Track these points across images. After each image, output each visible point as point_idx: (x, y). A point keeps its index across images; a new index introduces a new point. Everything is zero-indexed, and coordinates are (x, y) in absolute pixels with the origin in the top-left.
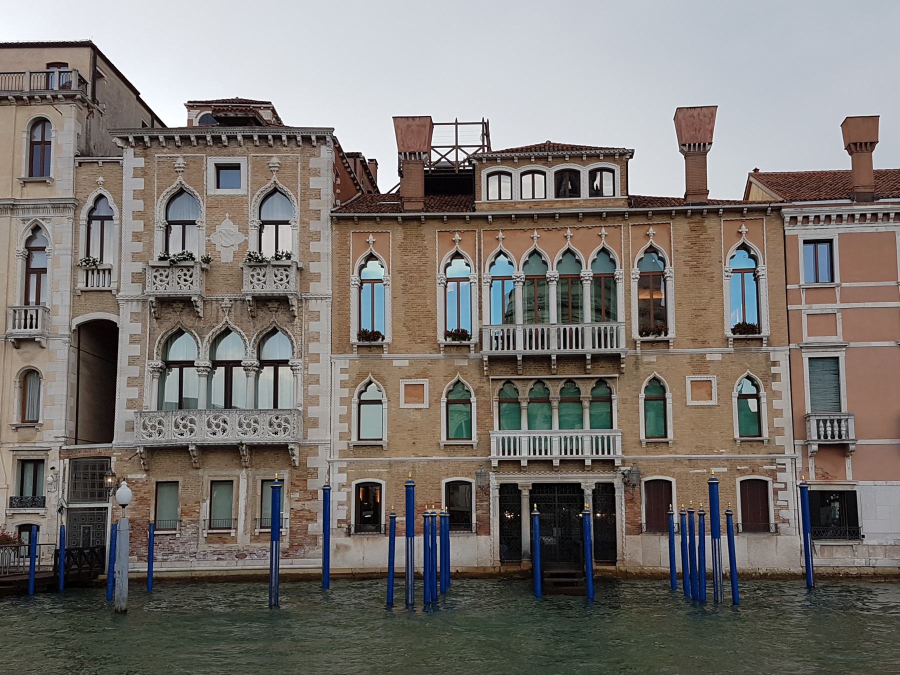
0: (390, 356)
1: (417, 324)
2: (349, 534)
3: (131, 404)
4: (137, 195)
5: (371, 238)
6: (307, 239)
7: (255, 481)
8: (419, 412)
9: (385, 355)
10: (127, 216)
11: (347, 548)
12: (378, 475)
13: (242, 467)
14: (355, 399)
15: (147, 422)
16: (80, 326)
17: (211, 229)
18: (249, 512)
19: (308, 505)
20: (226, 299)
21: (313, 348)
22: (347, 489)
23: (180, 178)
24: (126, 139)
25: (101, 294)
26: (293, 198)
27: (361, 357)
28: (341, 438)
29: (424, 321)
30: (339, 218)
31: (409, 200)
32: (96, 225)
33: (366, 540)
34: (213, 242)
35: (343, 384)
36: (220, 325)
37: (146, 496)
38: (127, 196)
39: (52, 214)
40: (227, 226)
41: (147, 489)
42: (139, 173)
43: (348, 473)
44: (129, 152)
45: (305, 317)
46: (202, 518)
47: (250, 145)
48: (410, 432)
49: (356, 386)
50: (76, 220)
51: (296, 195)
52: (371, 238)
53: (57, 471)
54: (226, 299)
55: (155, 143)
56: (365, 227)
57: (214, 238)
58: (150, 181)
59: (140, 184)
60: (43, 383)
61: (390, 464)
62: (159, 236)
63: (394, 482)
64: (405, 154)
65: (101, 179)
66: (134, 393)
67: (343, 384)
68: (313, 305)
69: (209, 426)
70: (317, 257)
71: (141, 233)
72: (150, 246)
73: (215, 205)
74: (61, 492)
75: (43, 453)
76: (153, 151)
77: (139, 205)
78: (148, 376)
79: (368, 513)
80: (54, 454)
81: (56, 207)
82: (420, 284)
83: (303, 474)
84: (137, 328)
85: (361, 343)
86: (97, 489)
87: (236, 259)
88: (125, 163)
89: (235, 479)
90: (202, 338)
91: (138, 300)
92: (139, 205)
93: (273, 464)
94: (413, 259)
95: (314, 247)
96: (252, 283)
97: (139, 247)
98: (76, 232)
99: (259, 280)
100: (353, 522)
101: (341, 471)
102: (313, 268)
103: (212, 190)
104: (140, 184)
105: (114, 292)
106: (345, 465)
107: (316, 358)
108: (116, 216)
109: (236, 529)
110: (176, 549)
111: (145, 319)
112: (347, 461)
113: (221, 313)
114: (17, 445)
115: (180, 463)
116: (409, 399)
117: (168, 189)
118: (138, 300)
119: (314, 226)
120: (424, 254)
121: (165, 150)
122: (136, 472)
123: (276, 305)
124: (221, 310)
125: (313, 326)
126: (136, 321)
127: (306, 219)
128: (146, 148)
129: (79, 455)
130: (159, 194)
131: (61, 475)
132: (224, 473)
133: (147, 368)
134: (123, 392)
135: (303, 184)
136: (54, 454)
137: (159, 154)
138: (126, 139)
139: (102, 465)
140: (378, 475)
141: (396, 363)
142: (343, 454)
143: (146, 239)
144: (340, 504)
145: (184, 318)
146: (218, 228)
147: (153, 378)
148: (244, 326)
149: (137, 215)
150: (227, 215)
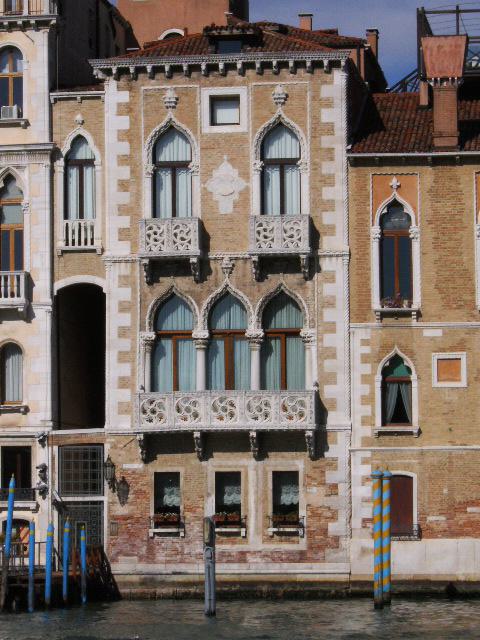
1: (451, 285)
3: (124, 383)
5: (394, 182)
6: (318, 184)
7: (265, 473)
12: (407, 467)
14: (379, 378)
16: (64, 291)
17: (207, 175)
18: (260, 507)
20: (227, 258)
21: (329, 315)
26: (301, 135)
28: (364, 422)
29: (460, 281)
30: (355, 158)
31: (441, 135)
32: (74, 172)
34: (209, 189)
35: (365, 359)
36: (219, 290)
37: (144, 488)
38: (110, 137)
39: (25, 161)
40: (225, 170)
42: (127, 109)
44: (111, 85)
48: (444, 417)
49: (379, 361)
51: (305, 131)
56: (387, 170)
57: (212, 186)
58: (136, 119)
59: (124, 122)
61: (422, 453)
62: (147, 184)
63: (427, 475)
65: (79, 117)
66: (125, 370)
67: (365, 359)
68: (326, 265)
70: (330, 205)
71: (127, 181)
72: (138, 196)
73: (210, 146)
77: (124, 148)
79: (398, 507)
81: (31, 152)
84: (126, 294)
85: (386, 309)
86: (89, 481)
88: (106, 98)
89: (242, 470)
90: (199, 305)
91: (127, 261)
92: (124, 148)
94: (446, 207)
95: (327, 193)
97: (125, 198)
101: (365, 461)
102: (326, 219)
103: (207, 129)
104: (124, 122)
106: (368, 454)
107: (331, 328)
111: (134, 283)
116: (443, 377)
117: (157, 128)
118: (127, 261)
119: (327, 168)
122: (132, 461)
125: (328, 289)
126: (126, 285)
129: (70, 441)
130: (146, 134)
133: (140, 341)
134: (114, 369)
137: (146, 85)
139: (94, 451)
140: (407, 467)
141: (427, 333)
142: (366, 441)
143: (133, 188)
146: (216, 174)
148: (248, 290)
149: (123, 160)
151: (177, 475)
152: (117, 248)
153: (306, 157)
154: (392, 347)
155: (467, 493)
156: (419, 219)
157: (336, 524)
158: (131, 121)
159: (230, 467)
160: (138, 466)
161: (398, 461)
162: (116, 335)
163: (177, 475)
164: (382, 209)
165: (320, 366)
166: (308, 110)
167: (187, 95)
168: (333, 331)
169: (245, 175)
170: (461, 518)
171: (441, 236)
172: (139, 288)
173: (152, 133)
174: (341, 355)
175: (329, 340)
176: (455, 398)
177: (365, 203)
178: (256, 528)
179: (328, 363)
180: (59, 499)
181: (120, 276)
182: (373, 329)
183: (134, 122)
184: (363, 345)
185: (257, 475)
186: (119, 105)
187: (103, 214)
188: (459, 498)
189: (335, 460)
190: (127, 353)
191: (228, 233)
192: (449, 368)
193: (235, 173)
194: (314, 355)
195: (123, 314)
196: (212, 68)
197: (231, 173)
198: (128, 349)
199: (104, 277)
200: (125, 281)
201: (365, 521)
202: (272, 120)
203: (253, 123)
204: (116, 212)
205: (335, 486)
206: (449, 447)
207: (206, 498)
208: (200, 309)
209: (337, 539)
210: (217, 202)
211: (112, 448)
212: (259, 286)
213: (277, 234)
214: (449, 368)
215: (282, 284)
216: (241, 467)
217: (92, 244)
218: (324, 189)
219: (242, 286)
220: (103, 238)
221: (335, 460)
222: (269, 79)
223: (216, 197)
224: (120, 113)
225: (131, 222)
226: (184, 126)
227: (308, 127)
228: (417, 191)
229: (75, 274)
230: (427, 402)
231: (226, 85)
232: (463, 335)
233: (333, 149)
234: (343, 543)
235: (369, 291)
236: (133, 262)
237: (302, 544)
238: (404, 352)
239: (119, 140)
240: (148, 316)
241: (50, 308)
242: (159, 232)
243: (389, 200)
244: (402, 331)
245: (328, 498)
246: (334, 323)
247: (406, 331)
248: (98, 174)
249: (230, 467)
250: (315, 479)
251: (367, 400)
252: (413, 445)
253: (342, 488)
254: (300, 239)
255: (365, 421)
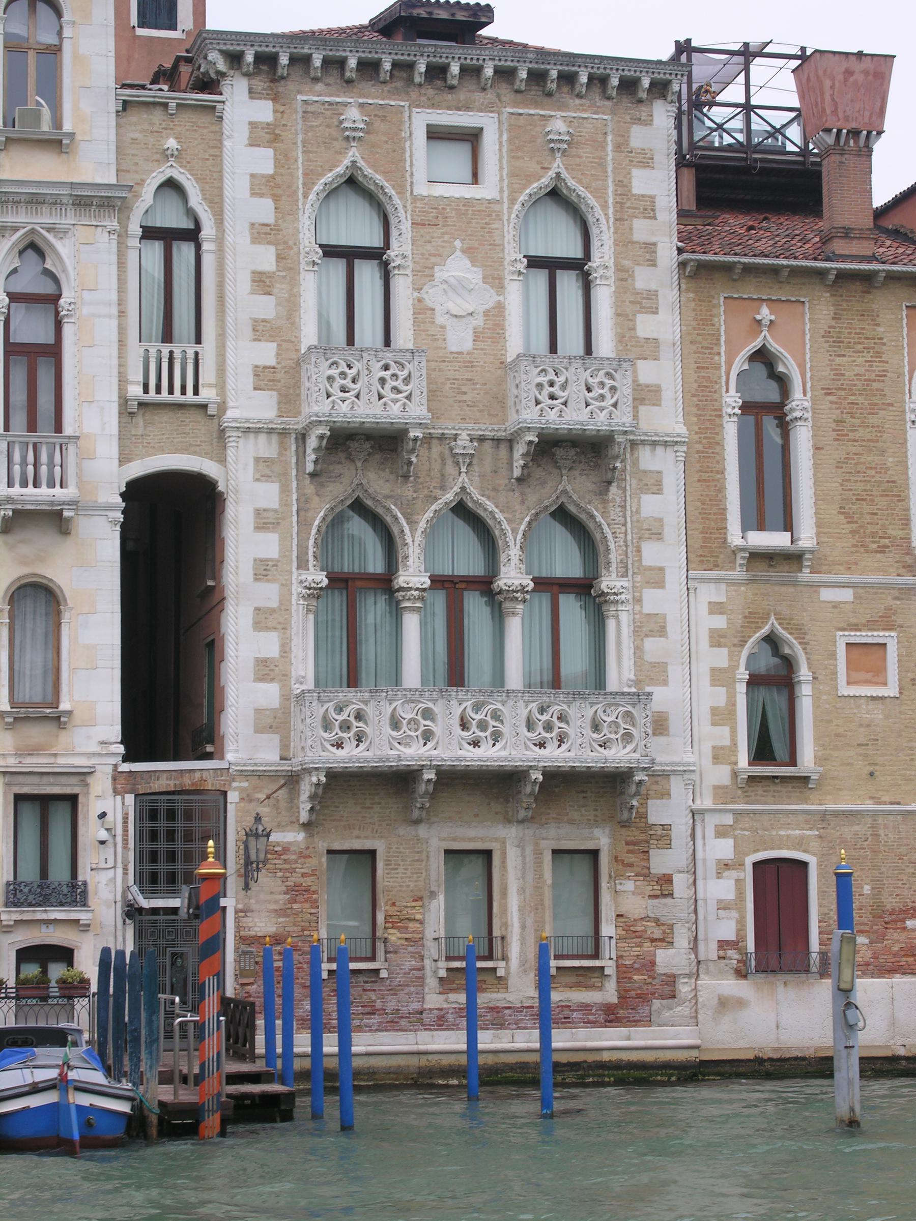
0: (816, 577)
1: (867, 508)
2: (741, 974)
3: (265, 670)
4: (263, 186)
7: (538, 853)
8: (879, 705)
9: (806, 575)
10: (238, 236)
11: (741, 1003)
13: (508, 821)
14: (743, 674)
15: (332, 714)
16: (131, 485)
17: (424, 274)
18: (530, 921)
19: (657, 908)
20: (464, 435)
21: (652, 554)
22: (734, 874)
23: (354, 154)
24: (235, 59)
25: (179, 414)
27: (751, 581)
29: (882, 502)
33: (780, 988)
34: (429, 303)
35: (717, 639)
37: (307, 882)
38: (236, 187)
39: (68, 218)
40: (458, 267)
41: (313, 862)
42: (265, 135)
43: (735, 838)
45: (631, 483)
46: (429, 934)
47: (504, 89)
49: (743, 643)
50: (122, 235)
51: (604, 207)
52: (765, 313)
53: (108, 816)
54: (464, 435)
55: (298, 70)
56: (749, 290)
57: (433, 296)
59: (263, 161)
60: (65, 618)
61: (824, 816)
64: (839, 132)
65: (172, 143)
66: (268, 645)
67: (717, 639)
69: (464, 726)
72: (291, 306)
73: (433, 216)
74: (120, 871)
75: (74, 780)
76: (291, 86)
78: (298, 607)
80: (101, 784)
82: (872, 420)
83: (644, 838)
87: (481, 345)
90: (412, 523)
93: (575, 815)
94: (855, 365)
95: (645, 326)
96: (538, 403)
97: (266, 307)
98: (121, 265)
99: (552, 397)
100: (751, 947)
101: (721, 832)
104: (263, 161)
105: (212, 410)
106: (729, 820)
107: (657, 578)
108: (208, 231)
109: (504, 958)
110: (379, 1004)
111: (285, 474)
112: (737, 813)
113: (450, 469)
114: (11, 761)
115: (377, 808)
116: (857, 676)
117: (329, 177)
118: (271, 431)
119: (644, 279)
120: (879, 354)
121: (319, 87)
123: (572, 452)
124: (449, 461)
127: (627, 263)
128: (276, 79)
129: (158, 785)
130: (308, 187)
131: (119, 831)
132: (472, 833)
133: (297, 589)
135: (619, 183)
136: (101, 784)
138: (235, 59)
140: (800, 844)
141: (827, 595)
142: (720, 792)
143: (281, 288)
144: (723, 906)
145: (372, 475)
146: (440, 274)
147: (309, 611)
149: (262, 233)
150: (458, 243)
151: (372, 853)
152: (249, 405)
153: (603, 256)
154: (768, 618)
155: (906, 892)
156: (809, 385)
157: (671, 952)
158: (276, 160)
159: (470, 840)
160: (293, 837)
161: (782, 833)
162: (251, 577)
163: (372, 853)
164: (740, 363)
165: (638, 650)
166: (610, 169)
167: (384, 119)
168: (660, 584)
169: (496, 282)
170: (896, 940)
171: (847, 418)
172: (294, 485)
173: (318, 187)
174: (675, 630)
175: (653, 600)
176: (877, 714)
177: (711, 348)
178: (523, 963)
179: (650, 644)
180: (145, 903)
181: (257, 460)
182: (731, 583)
183: (283, 160)
184: (711, 612)
185: (523, 856)
186: (253, 125)
187: (222, 336)
188: (890, 902)
189: (667, 827)
190: (272, 611)
191: (464, 389)
192: (865, 659)
193: (471, 274)
194: (626, 630)
195: (261, 536)
196: (437, 72)
197: (469, 276)
198: (274, 604)
199: (222, 460)
200: (265, 469)
201: (723, 945)
202: (545, 181)
203: (510, 184)
204: (248, 331)
205: (667, 880)
206: (870, 806)
207: (426, 901)
208: (413, 531)
209: (671, 980)
210: (443, 327)
211: (242, 799)
212: (522, 494)
213: (576, 392)
214: (865, 659)
215: (565, 492)
216: (496, 840)
217: (196, 392)
218: (640, 318)
219: (493, 492)
220: (221, 385)
221: (667, 827)
222: (537, 105)
223: (440, 319)
224: (253, 143)
225: (278, 354)
226: (379, 178)
227: (611, 200)
228: (804, 337)
229: (163, 452)
230: (830, 721)
231: (459, 109)
232: (889, 601)
233: (654, 244)
234: (684, 988)
235: (723, 512)
236: (283, 433)
237: (609, 993)
238: (784, 629)
239: (254, 194)
240: (311, 542)
241: (120, 517)
242: (352, 373)
243: (756, 344)
244: (783, 589)
245: (655, 901)
246: (661, 569)
247: (791, 589)
248: (208, 261)
249: (470, 840)
250: (631, 865)
251: (723, 716)
252: (806, 801)
253: (680, 883)
254: (615, 405)
255: (720, 755)
